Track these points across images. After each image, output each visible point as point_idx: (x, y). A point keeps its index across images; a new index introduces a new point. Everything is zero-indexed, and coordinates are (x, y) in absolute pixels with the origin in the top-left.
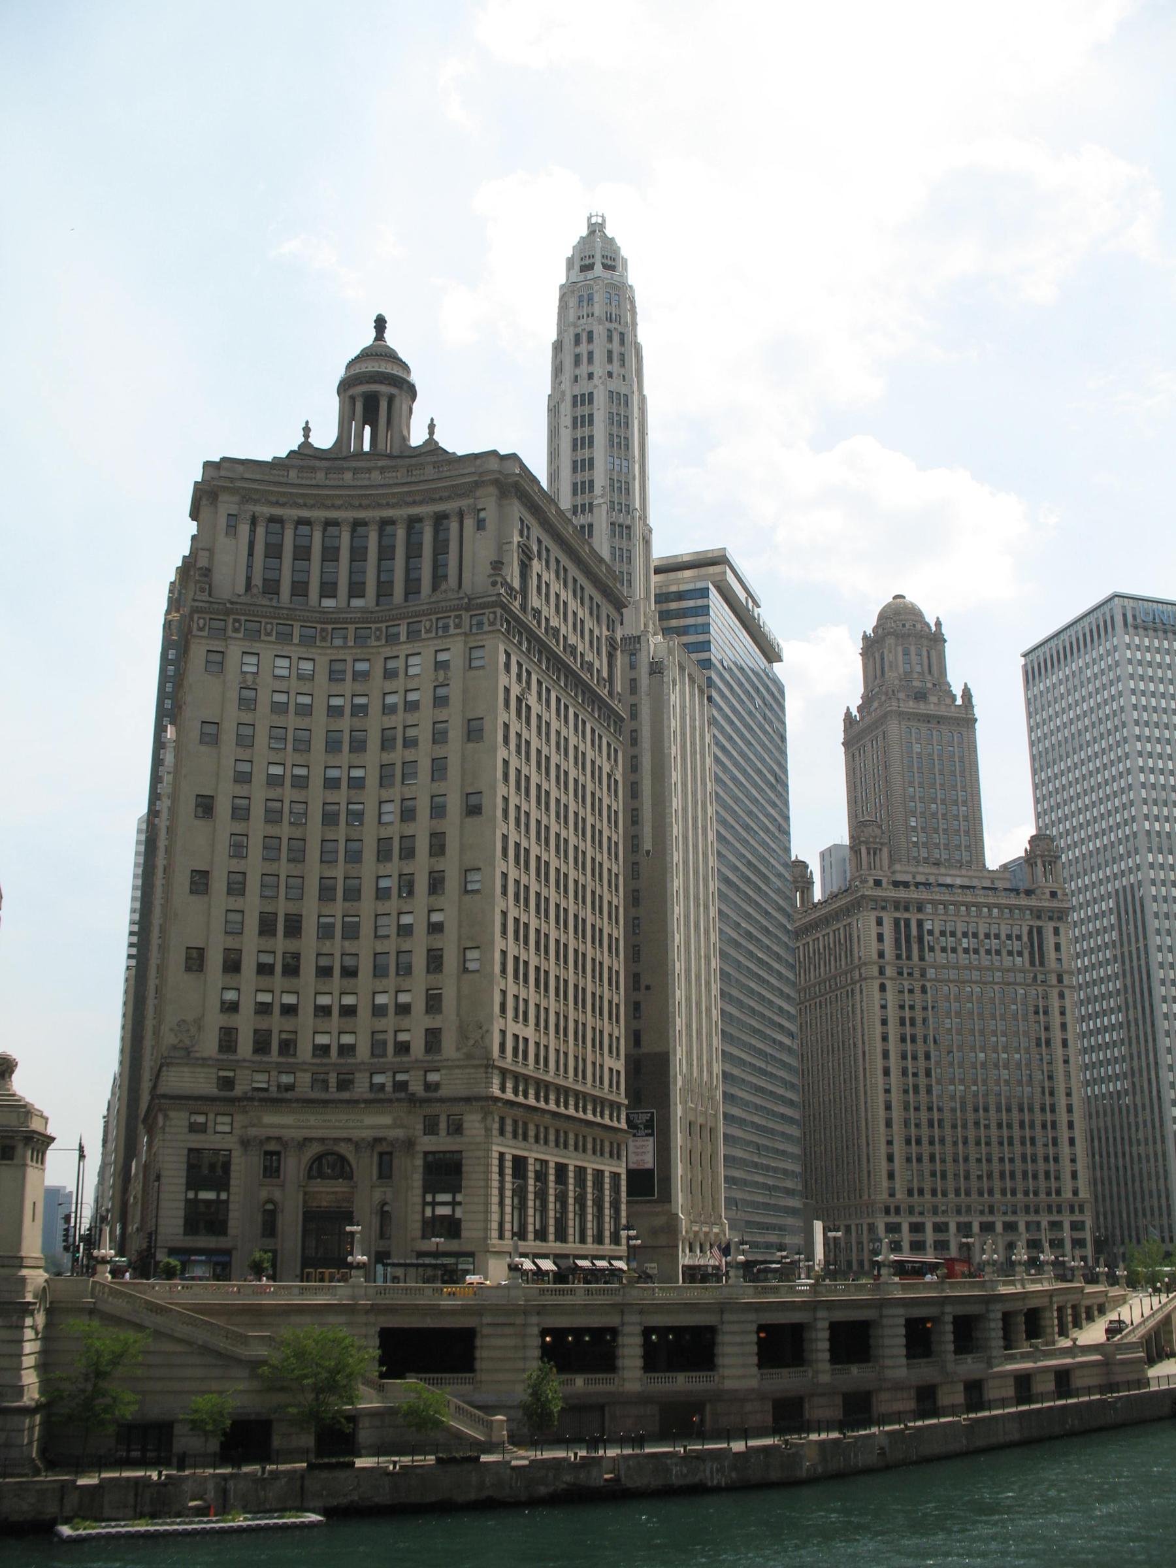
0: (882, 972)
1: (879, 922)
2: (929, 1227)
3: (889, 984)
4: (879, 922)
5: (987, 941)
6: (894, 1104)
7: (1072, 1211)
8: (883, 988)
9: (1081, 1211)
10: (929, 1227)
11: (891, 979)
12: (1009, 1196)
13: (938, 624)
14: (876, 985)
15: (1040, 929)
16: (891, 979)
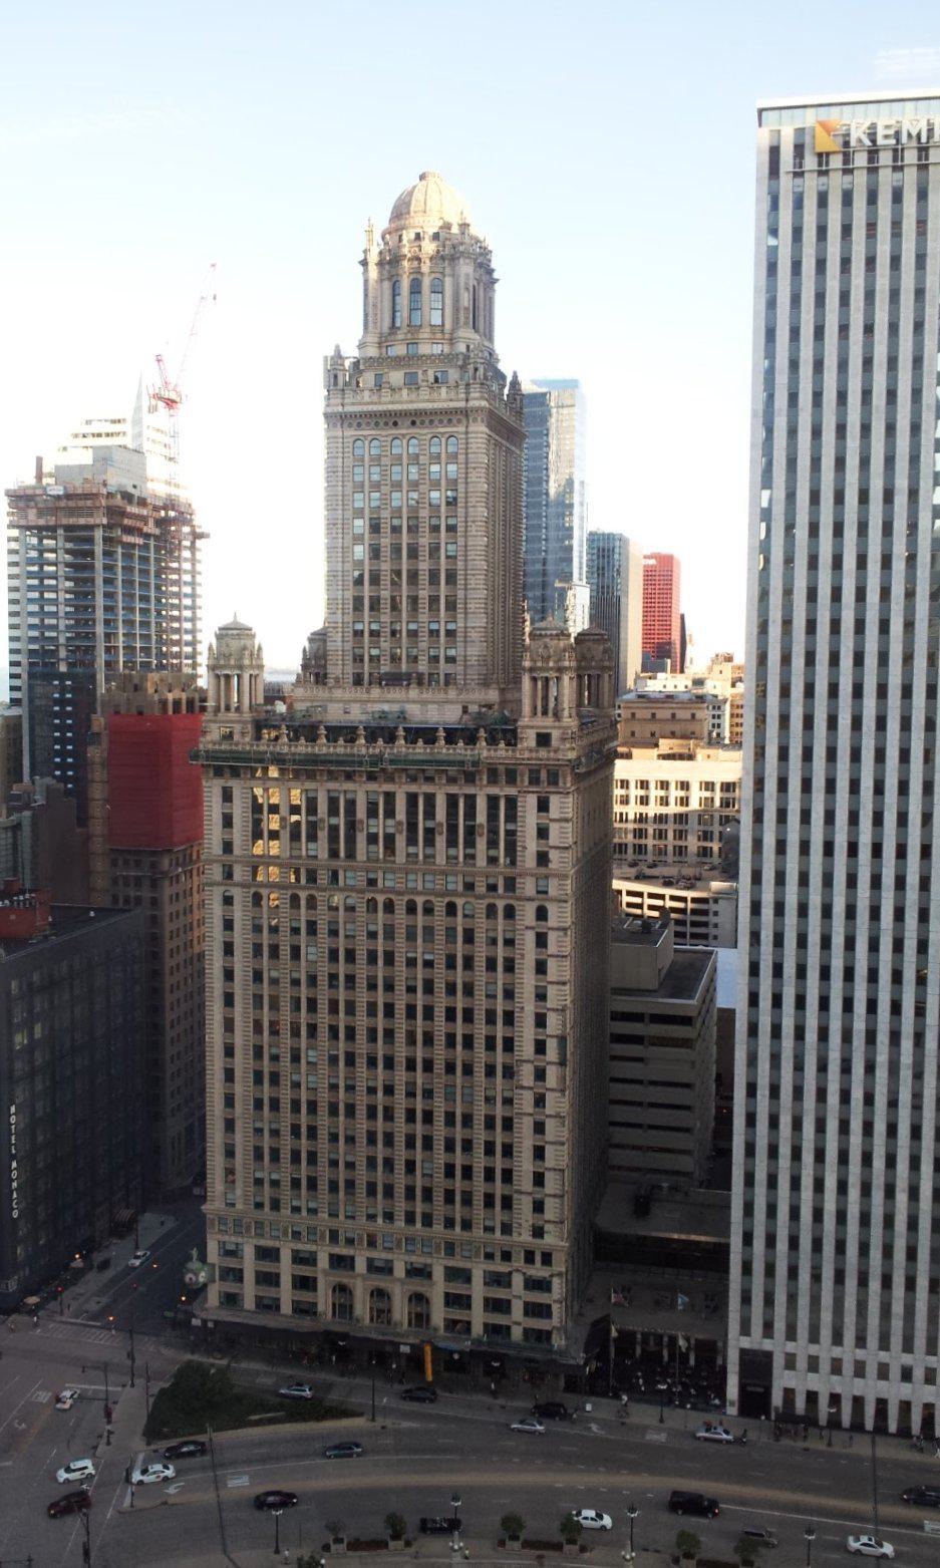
0: (229, 875)
1: (227, 796)
2: (286, 1256)
3: (237, 893)
4: (227, 796)
5: (391, 830)
6: (238, 1074)
7: (529, 1257)
8: (228, 901)
9: (547, 1259)
10: (286, 1256)
11: (243, 885)
12: (419, 1225)
13: (464, 226)
14: (217, 894)
15: (512, 803)
16: (243, 885)
